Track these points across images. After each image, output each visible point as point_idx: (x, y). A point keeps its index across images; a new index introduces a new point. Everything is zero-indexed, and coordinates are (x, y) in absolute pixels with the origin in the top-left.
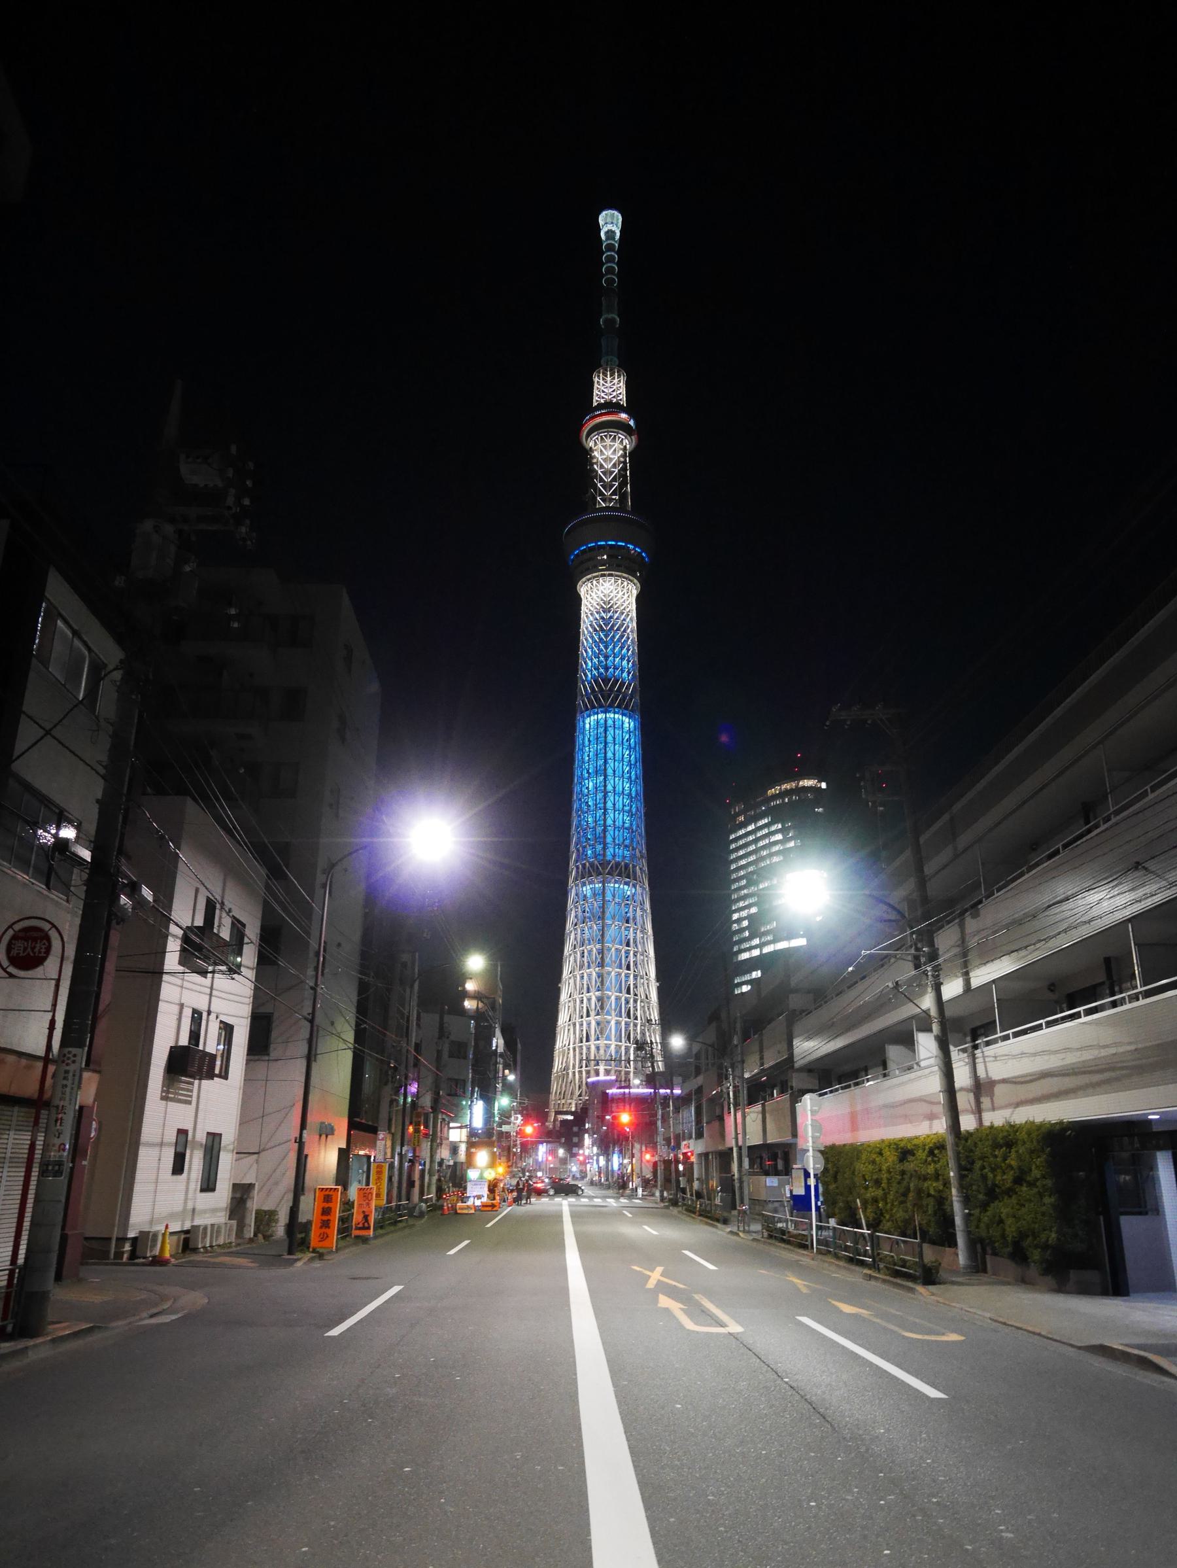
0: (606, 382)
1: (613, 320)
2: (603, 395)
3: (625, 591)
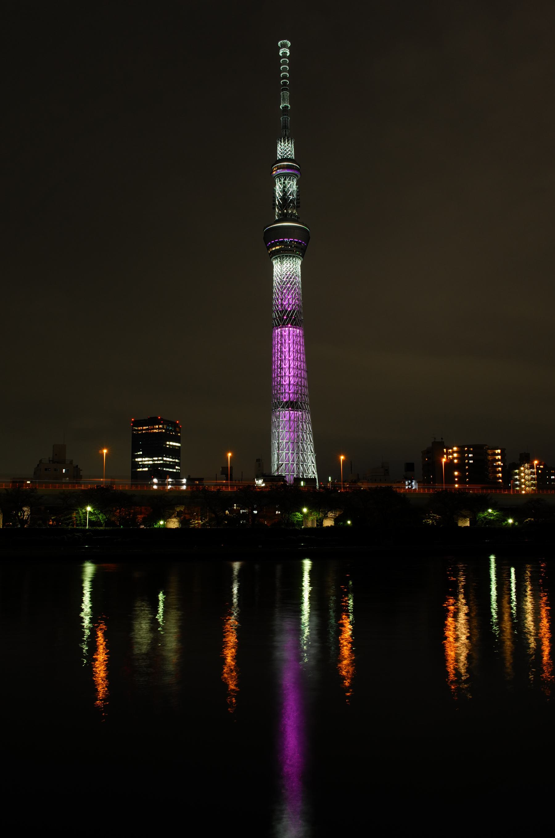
0: (281, 146)
2: (280, 153)
3: (291, 262)
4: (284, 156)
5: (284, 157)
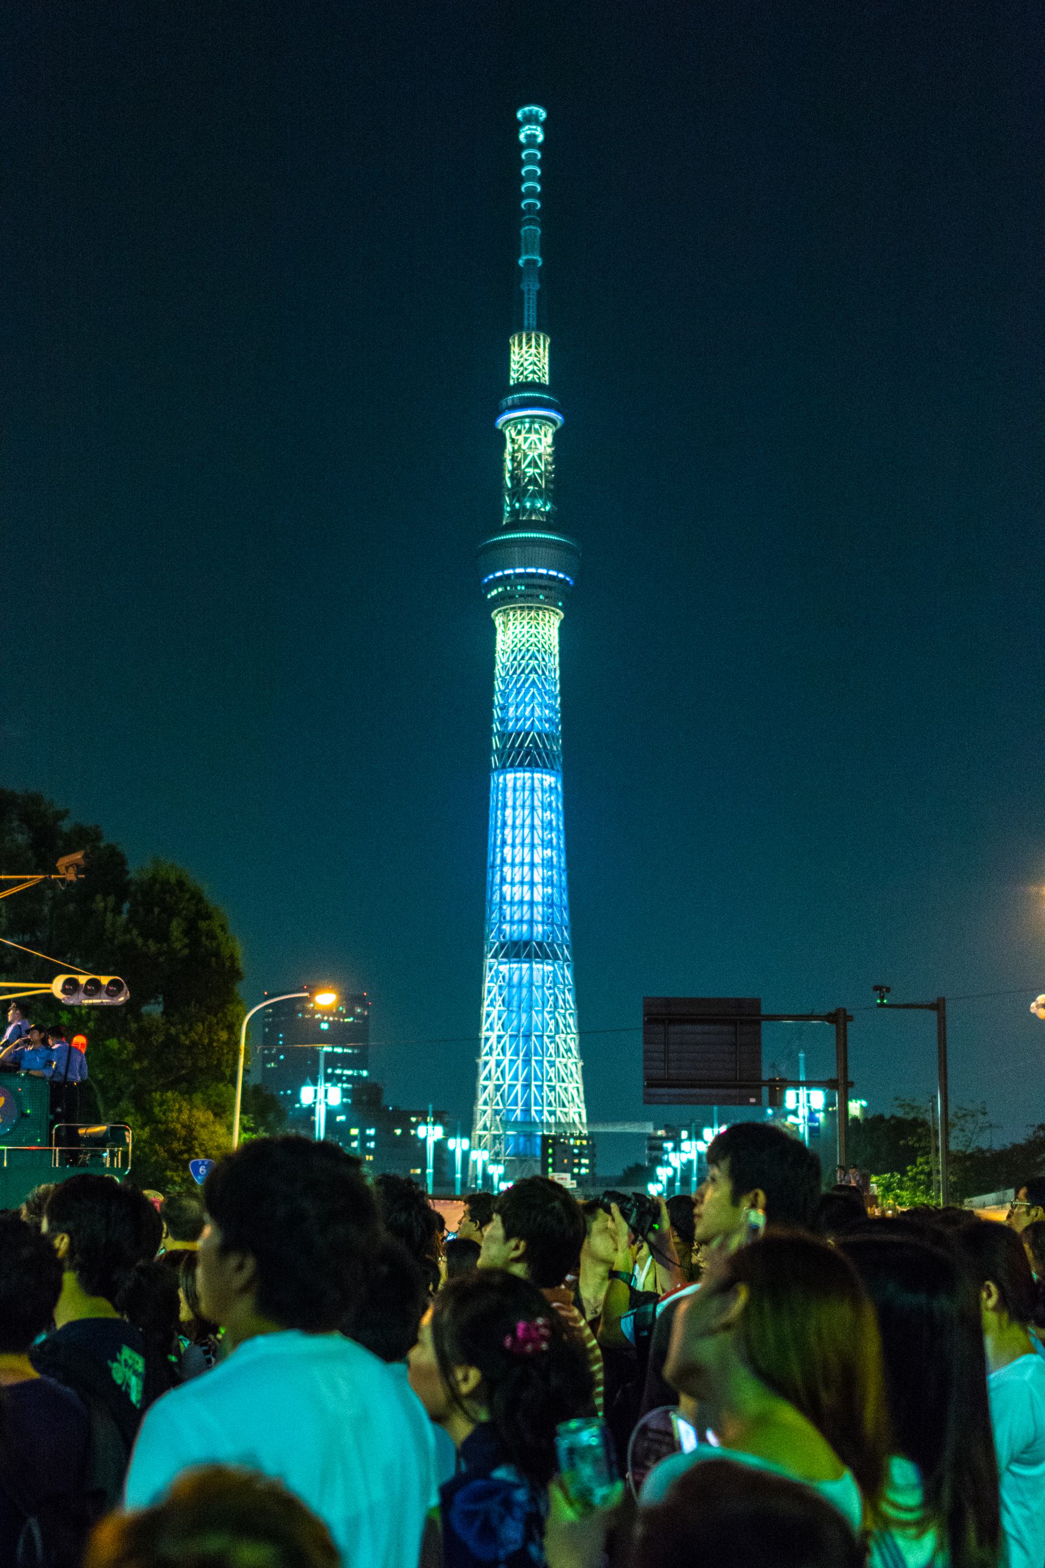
1: (535, 262)
4: (527, 377)
5: (529, 379)
